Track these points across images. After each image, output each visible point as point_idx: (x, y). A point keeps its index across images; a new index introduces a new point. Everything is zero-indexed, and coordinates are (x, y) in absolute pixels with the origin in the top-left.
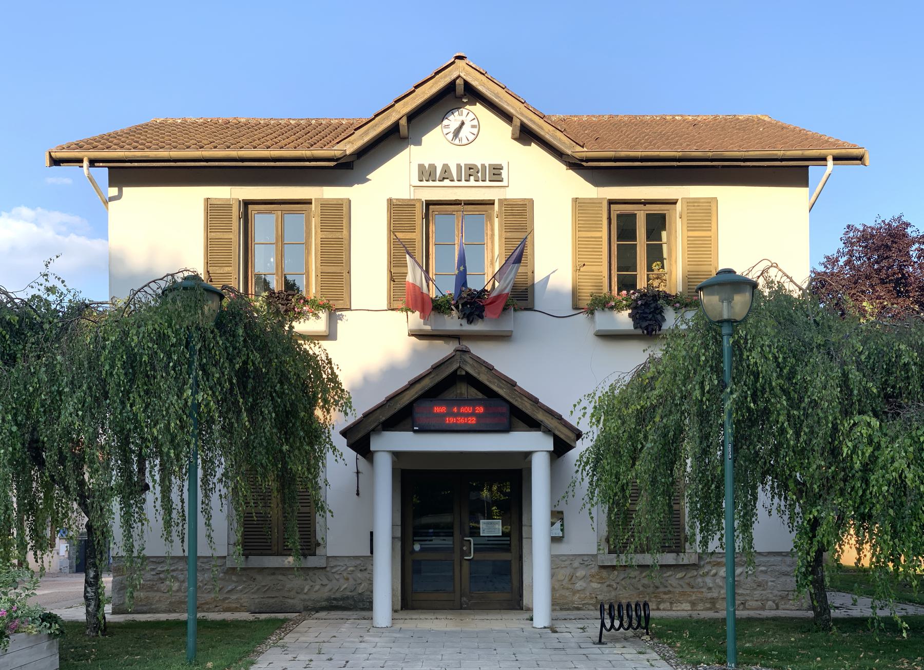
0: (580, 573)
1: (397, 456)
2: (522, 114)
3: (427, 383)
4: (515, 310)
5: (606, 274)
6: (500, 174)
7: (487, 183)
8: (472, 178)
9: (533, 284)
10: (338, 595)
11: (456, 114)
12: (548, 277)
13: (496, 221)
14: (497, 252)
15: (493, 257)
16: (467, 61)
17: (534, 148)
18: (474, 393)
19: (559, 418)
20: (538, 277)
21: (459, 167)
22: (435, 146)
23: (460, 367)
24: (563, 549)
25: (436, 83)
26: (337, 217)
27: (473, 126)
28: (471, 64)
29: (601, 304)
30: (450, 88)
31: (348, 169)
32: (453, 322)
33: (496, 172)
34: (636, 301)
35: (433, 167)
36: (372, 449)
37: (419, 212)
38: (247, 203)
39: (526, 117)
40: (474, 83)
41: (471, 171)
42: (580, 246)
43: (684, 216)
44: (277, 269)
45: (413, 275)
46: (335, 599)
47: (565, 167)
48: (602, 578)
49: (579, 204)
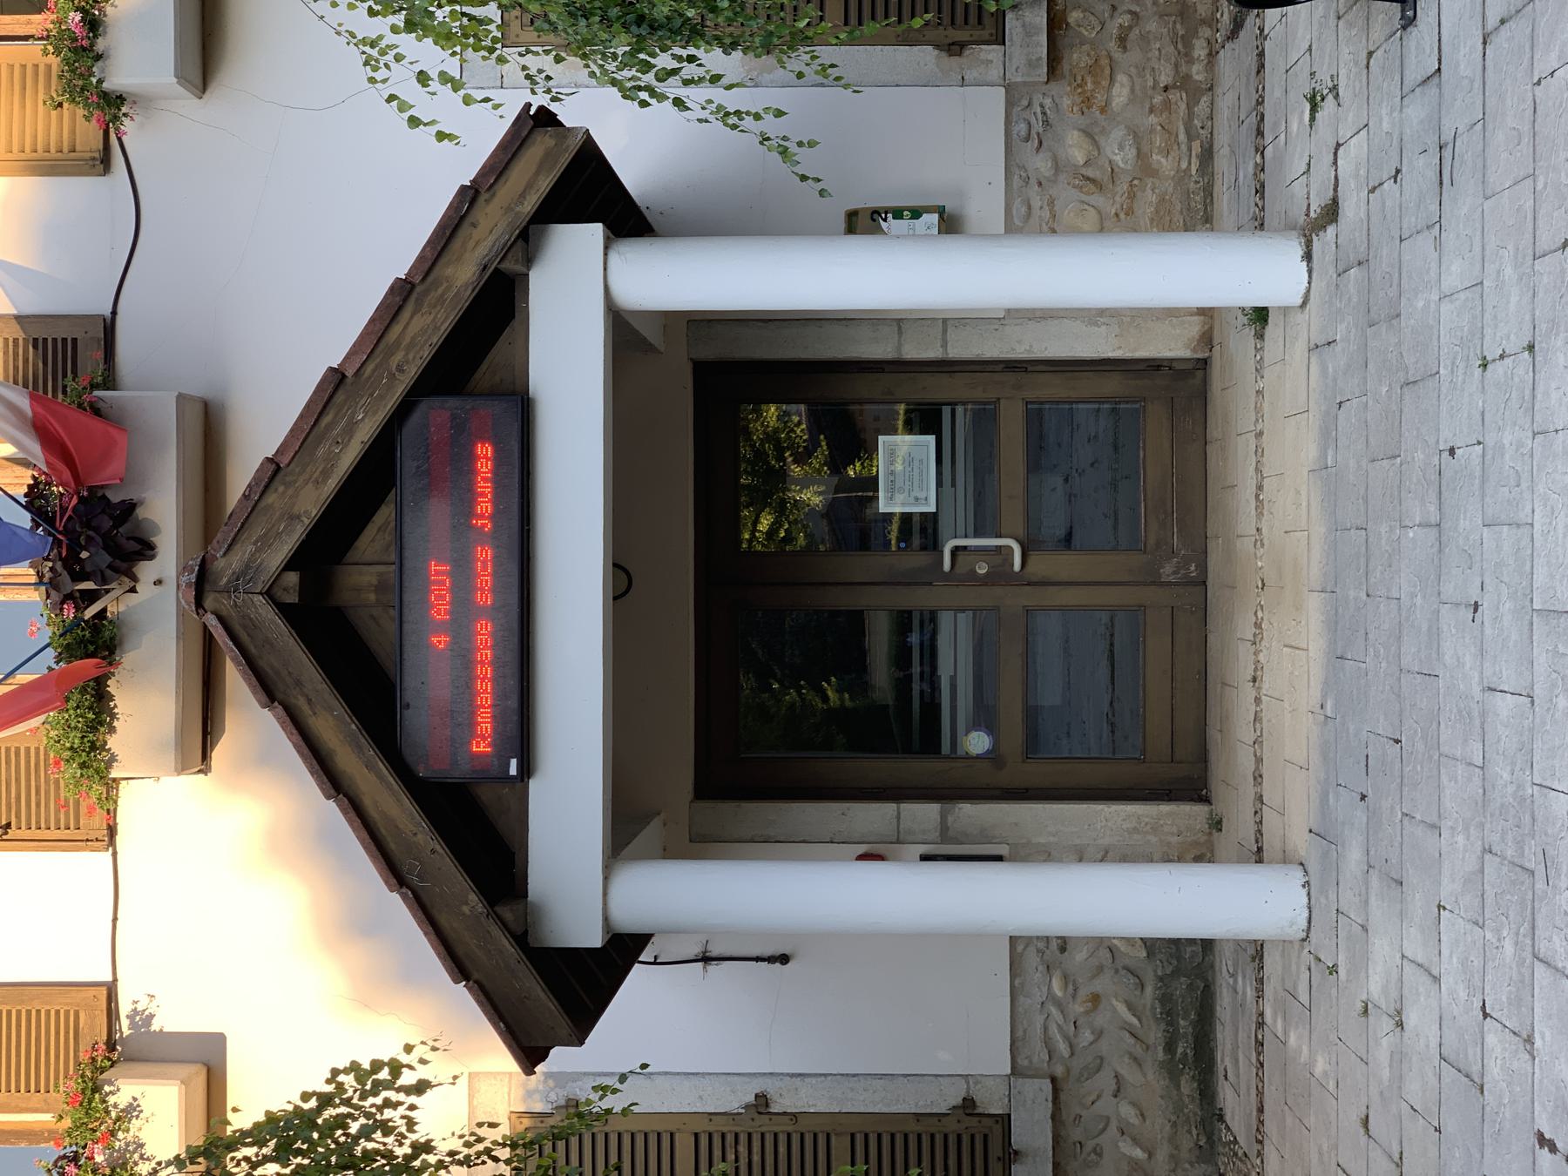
0: (1075, 150)
1: (629, 828)
3: (334, 724)
4: (109, 380)
9: (19, 319)
10: (1155, 1035)
18: (372, 540)
19: (470, 196)
23: (269, 594)
24: (986, 202)
36: (597, 942)
46: (1170, 1047)
48: (1094, 69)
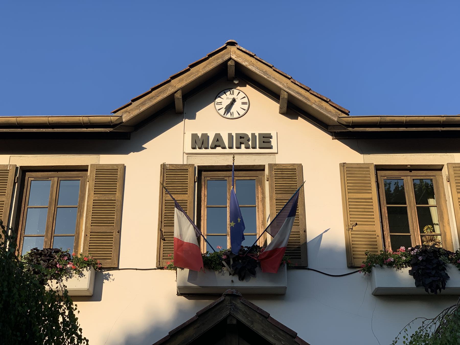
2: (289, 88)
4: (289, 268)
5: (379, 232)
6: (270, 142)
7: (258, 150)
8: (243, 146)
9: (306, 243)
11: (228, 93)
12: (321, 235)
13: (267, 184)
14: (268, 213)
15: (264, 218)
16: (238, 46)
17: (301, 123)
20: (311, 234)
21: (230, 136)
22: (209, 119)
23: (230, 315)
25: (209, 63)
26: (113, 180)
27: (243, 103)
28: (241, 48)
29: (377, 261)
30: (223, 68)
31: (126, 136)
32: (225, 279)
33: (266, 140)
34: (416, 256)
35: (205, 136)
37: (191, 177)
38: (25, 170)
39: (293, 91)
40: (245, 64)
41: (242, 139)
42: (352, 207)
43: (452, 179)
44: (47, 231)
45: (184, 231)
47: (330, 137)
49: (346, 169)
